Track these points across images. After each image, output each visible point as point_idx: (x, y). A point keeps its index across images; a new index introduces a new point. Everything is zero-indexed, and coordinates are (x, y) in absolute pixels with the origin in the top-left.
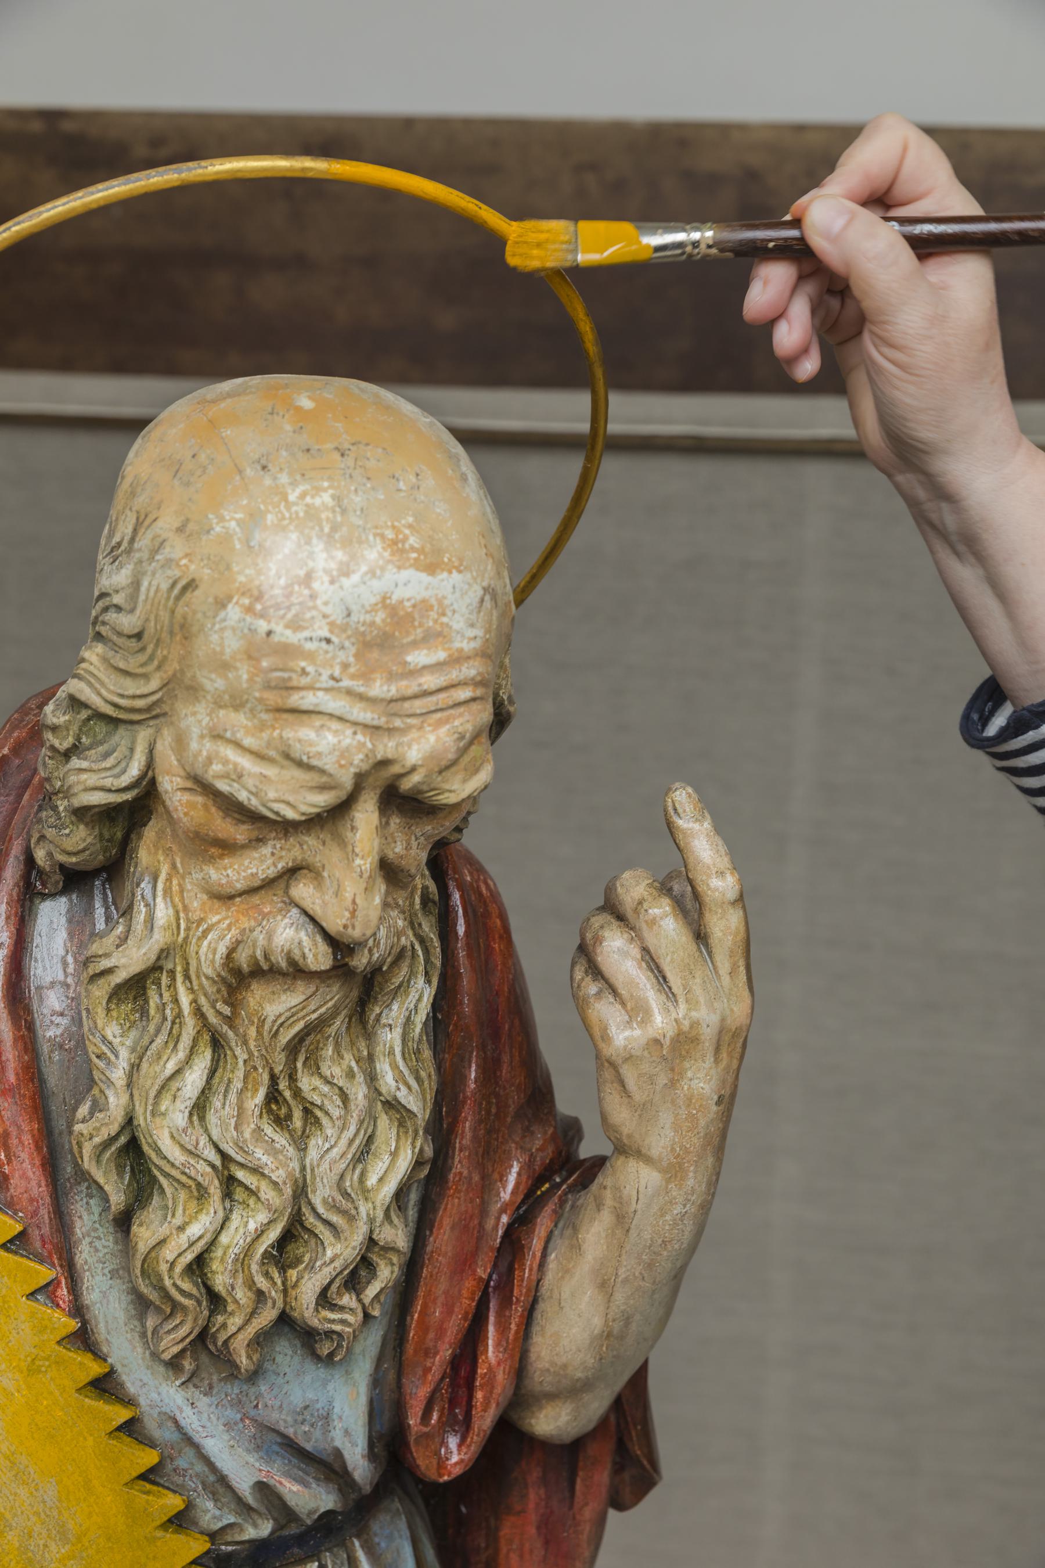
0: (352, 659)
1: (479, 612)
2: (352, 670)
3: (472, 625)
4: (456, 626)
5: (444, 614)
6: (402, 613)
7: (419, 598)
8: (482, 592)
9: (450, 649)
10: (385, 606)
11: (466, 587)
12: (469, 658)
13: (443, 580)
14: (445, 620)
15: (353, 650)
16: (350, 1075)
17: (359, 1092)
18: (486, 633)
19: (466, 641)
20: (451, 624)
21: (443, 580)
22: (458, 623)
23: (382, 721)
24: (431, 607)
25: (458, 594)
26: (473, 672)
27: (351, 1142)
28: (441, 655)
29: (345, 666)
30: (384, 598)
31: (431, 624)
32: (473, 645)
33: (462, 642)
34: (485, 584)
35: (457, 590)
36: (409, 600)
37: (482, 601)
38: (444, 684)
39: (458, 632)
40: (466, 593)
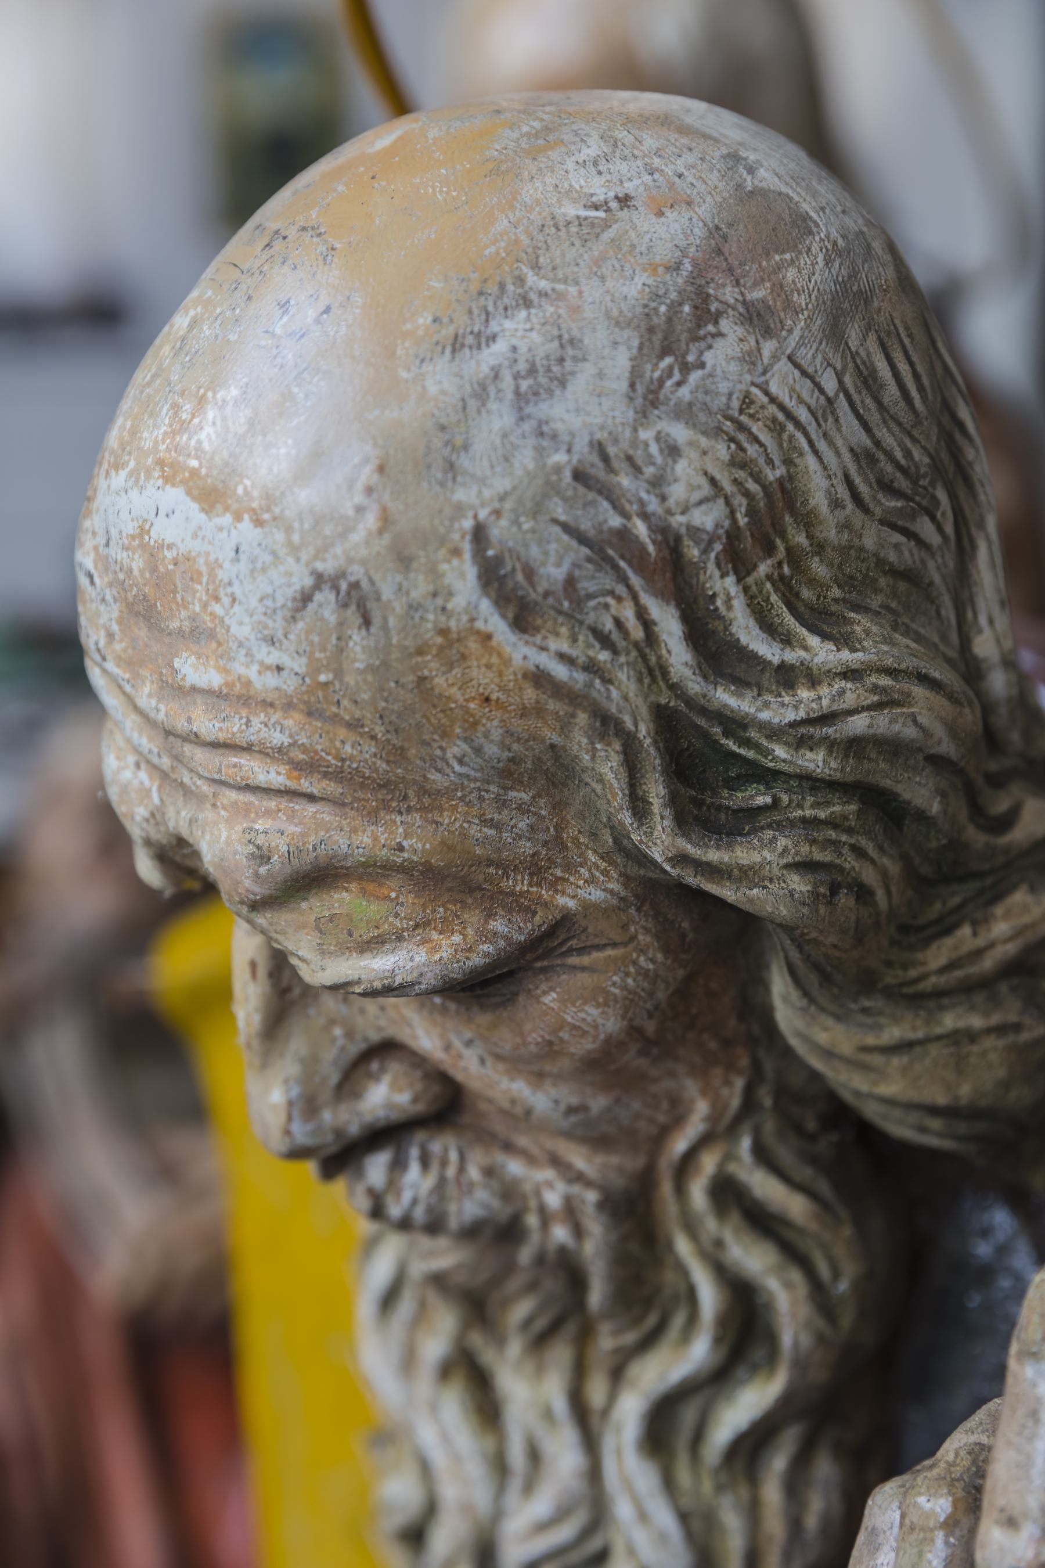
0: (115, 628)
1: (294, 618)
2: (118, 647)
3: (272, 641)
4: (234, 629)
5: (217, 599)
6: (162, 569)
7: (183, 549)
8: (309, 582)
9: (227, 671)
10: (143, 546)
11: (267, 558)
12: (268, 705)
13: (220, 529)
14: (217, 609)
15: (115, 610)
16: (548, 1415)
17: (565, 1457)
18: (315, 668)
19: (255, 668)
20: (227, 620)
21: (220, 529)
22: (241, 626)
23: (165, 762)
24: (195, 577)
25: (243, 566)
26: (278, 738)
27: (542, 1527)
28: (213, 679)
29: (110, 636)
30: (143, 531)
31: (197, 608)
32: (272, 681)
33: (247, 666)
34: (327, 566)
35: (243, 557)
36: (170, 547)
37: (305, 598)
38: (222, 737)
39: (241, 645)
40: (264, 570)
